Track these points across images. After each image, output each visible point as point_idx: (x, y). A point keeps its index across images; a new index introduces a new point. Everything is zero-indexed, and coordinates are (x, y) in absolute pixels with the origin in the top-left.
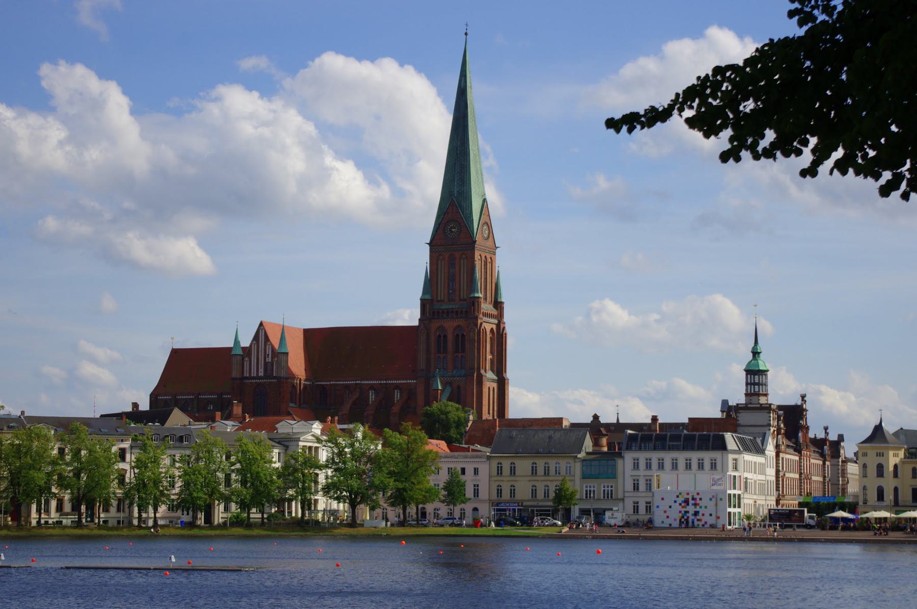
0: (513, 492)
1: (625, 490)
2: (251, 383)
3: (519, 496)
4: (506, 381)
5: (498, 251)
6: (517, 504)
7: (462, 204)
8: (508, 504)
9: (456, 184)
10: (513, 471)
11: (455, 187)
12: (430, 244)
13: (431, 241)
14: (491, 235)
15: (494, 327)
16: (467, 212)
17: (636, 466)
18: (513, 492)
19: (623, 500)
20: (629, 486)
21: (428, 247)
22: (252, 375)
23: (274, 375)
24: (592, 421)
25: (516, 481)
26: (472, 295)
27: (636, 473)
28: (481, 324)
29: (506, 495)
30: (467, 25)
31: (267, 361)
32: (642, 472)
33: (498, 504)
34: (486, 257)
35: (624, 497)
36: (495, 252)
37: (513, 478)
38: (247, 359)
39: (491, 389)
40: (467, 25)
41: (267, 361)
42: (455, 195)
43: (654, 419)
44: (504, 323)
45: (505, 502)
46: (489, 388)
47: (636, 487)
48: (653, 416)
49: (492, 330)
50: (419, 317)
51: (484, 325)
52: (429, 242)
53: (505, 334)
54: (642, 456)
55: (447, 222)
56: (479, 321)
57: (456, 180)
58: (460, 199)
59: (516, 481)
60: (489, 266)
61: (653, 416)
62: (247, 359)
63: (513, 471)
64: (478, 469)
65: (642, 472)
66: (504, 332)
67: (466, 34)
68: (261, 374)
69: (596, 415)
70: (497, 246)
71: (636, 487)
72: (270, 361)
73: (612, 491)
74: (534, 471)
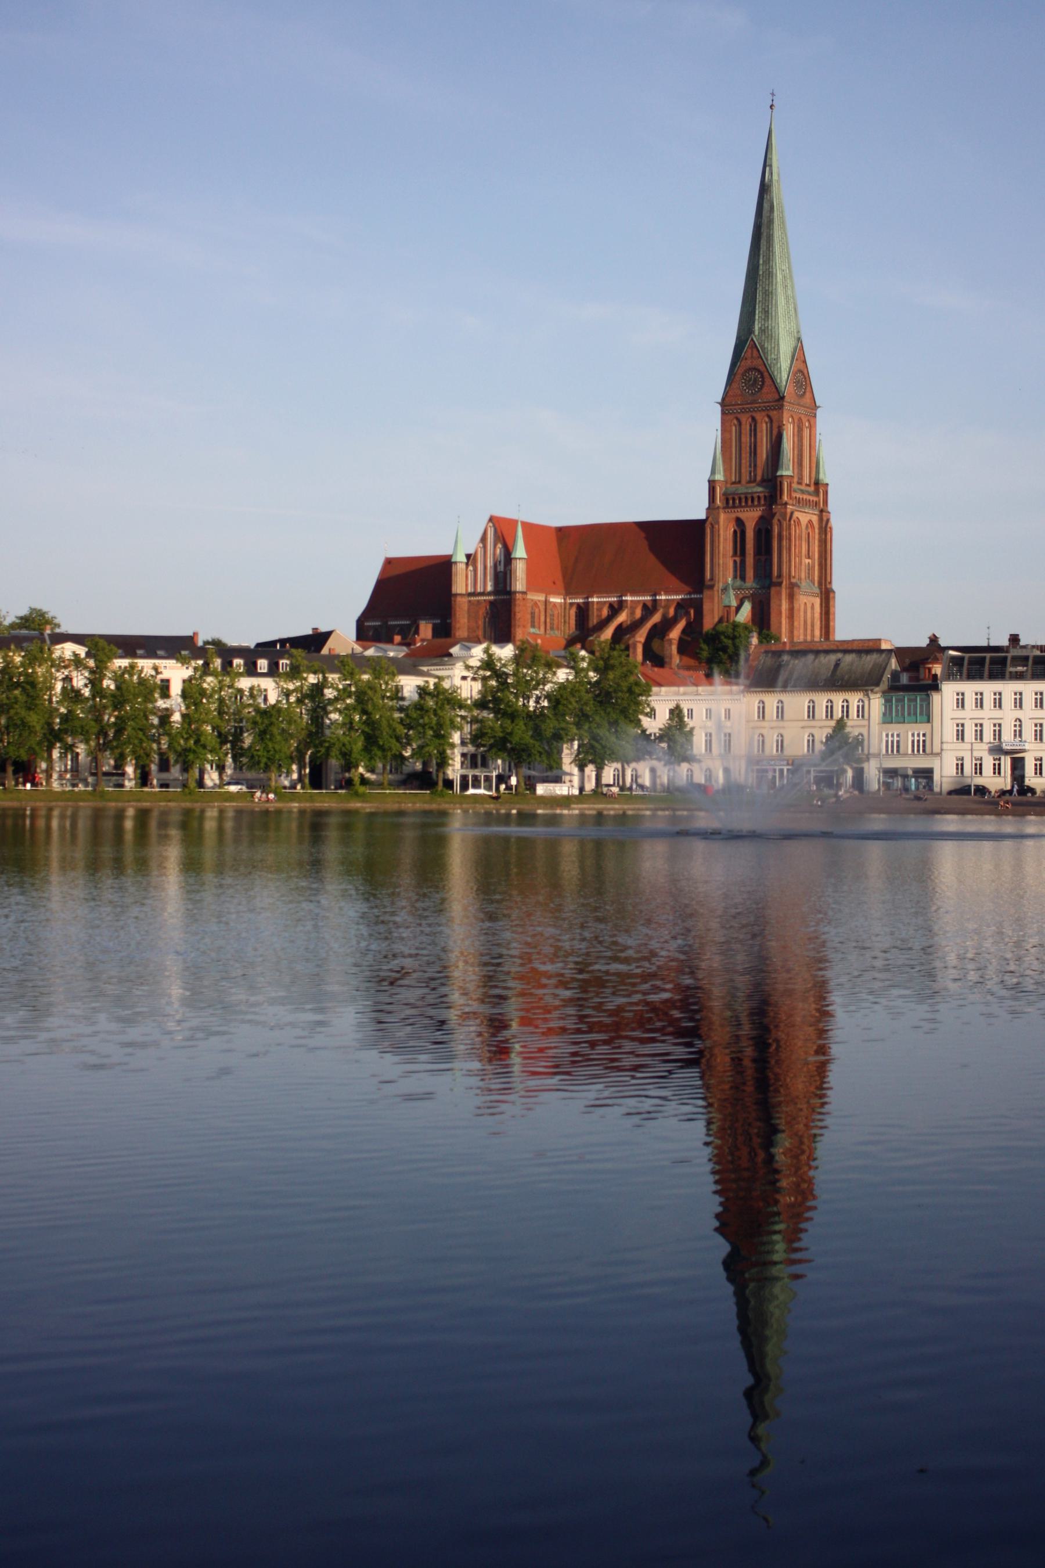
0: (781, 745)
1: (944, 740)
2: (478, 601)
3: (790, 751)
4: (831, 595)
5: (819, 412)
6: (785, 762)
7: (766, 346)
8: (773, 763)
9: (757, 317)
10: (781, 712)
11: (756, 322)
12: (723, 404)
13: (723, 399)
14: (808, 388)
15: (815, 519)
16: (773, 356)
17: (961, 703)
18: (781, 745)
19: (939, 754)
20: (950, 732)
21: (719, 408)
22: (479, 590)
23: (508, 589)
24: (928, 645)
25: (783, 727)
26: (779, 473)
27: (960, 714)
28: (792, 514)
29: (771, 749)
30: (773, 94)
31: (499, 570)
32: (970, 710)
33: (758, 762)
34: (800, 420)
35: (942, 750)
36: (815, 414)
37: (781, 724)
38: (471, 568)
39: (809, 606)
40: (773, 94)
41: (499, 570)
42: (757, 333)
43: (1014, 639)
44: (829, 513)
45: (772, 758)
46: (805, 603)
47: (961, 735)
48: (1011, 635)
49: (810, 522)
50: (707, 505)
51: (796, 514)
52: (720, 400)
53: (831, 528)
54: (970, 688)
55: (746, 371)
56: (789, 511)
57: (757, 312)
58: (763, 338)
59: (783, 727)
60: (806, 433)
61: (1011, 635)
62: (471, 568)
63: (781, 712)
64: (729, 710)
65: (970, 710)
66: (829, 525)
67: (771, 107)
68: (489, 588)
69: (934, 635)
70: (817, 405)
71: (961, 735)
72: (502, 570)
73: (924, 741)
74: (812, 713)
